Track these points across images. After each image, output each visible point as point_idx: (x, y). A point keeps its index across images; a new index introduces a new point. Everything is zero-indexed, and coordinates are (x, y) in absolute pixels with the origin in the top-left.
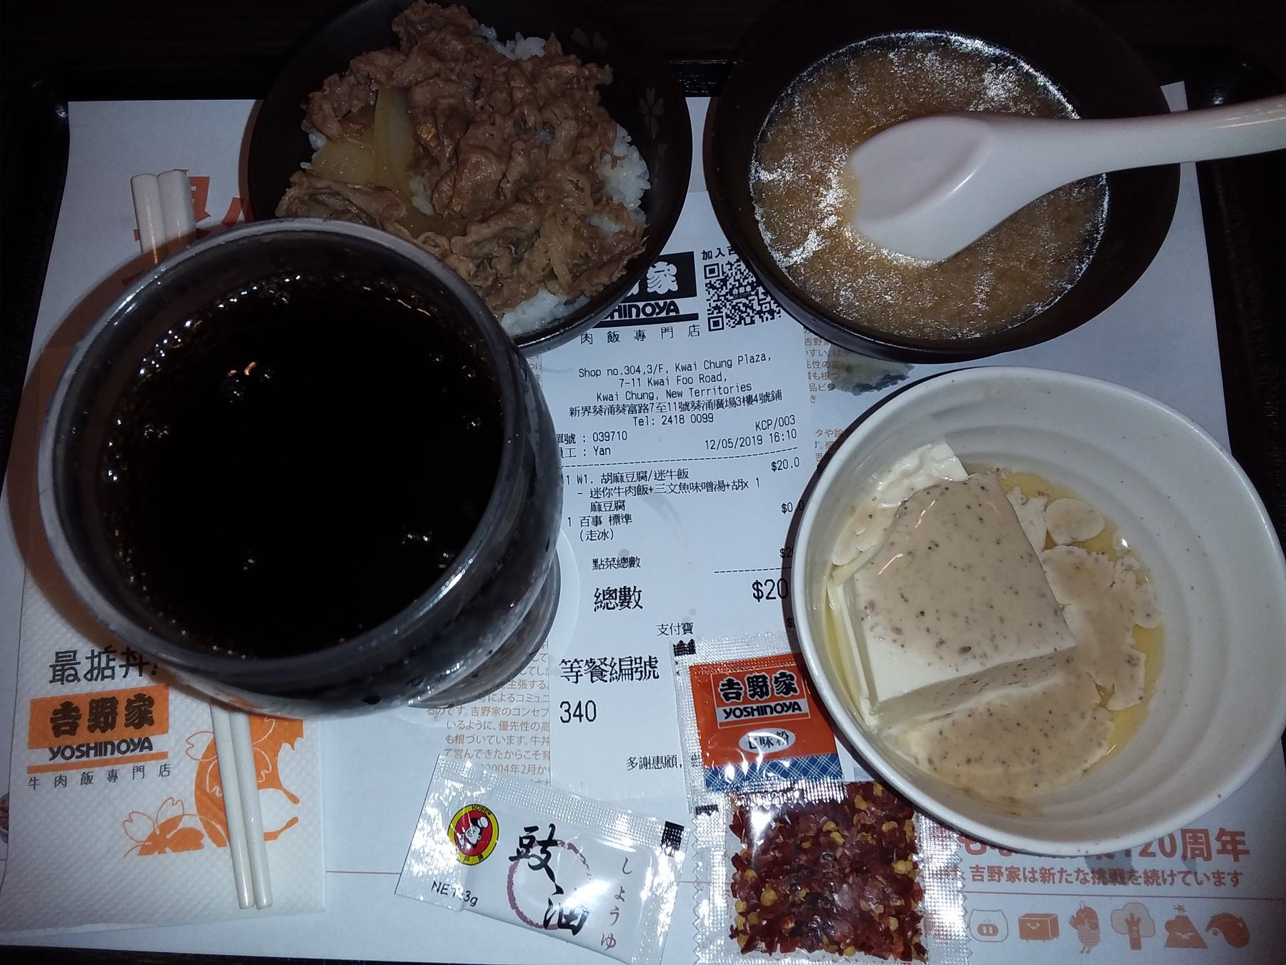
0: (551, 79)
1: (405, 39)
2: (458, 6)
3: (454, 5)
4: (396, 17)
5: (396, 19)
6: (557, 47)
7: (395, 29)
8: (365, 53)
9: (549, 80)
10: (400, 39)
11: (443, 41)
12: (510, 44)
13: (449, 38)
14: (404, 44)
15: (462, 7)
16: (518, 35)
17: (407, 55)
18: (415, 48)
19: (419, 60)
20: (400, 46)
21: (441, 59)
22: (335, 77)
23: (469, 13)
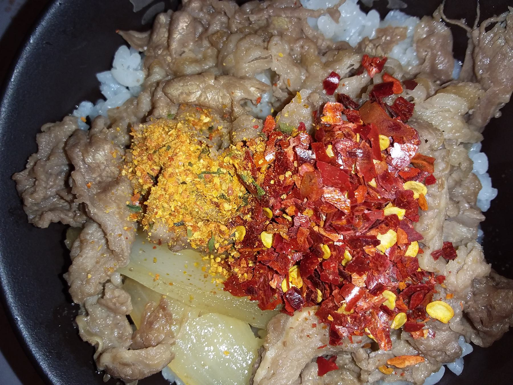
0: (184, 52)
1: (62, 216)
2: (40, 132)
3: (38, 135)
4: (27, 216)
5: (31, 217)
6: (137, 37)
7: (44, 224)
8: (65, 276)
9: (184, 55)
10: (60, 223)
11: (90, 169)
12: (105, 91)
13: (89, 160)
14: (68, 219)
15: (44, 128)
16: (102, 76)
17: (91, 220)
18: (93, 211)
19: (108, 211)
20: (68, 226)
21: (117, 181)
22: (82, 322)
23: (54, 122)
